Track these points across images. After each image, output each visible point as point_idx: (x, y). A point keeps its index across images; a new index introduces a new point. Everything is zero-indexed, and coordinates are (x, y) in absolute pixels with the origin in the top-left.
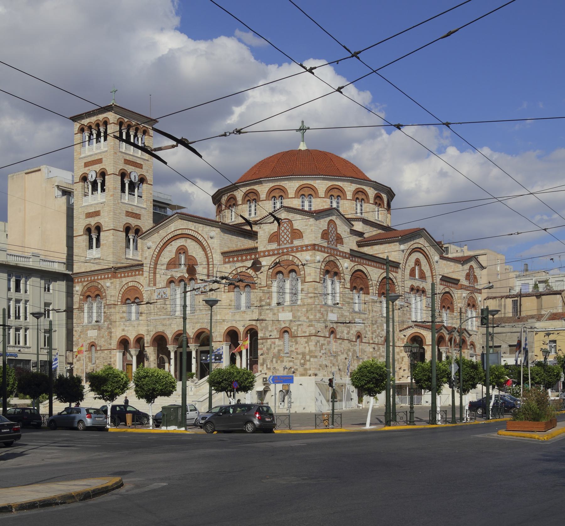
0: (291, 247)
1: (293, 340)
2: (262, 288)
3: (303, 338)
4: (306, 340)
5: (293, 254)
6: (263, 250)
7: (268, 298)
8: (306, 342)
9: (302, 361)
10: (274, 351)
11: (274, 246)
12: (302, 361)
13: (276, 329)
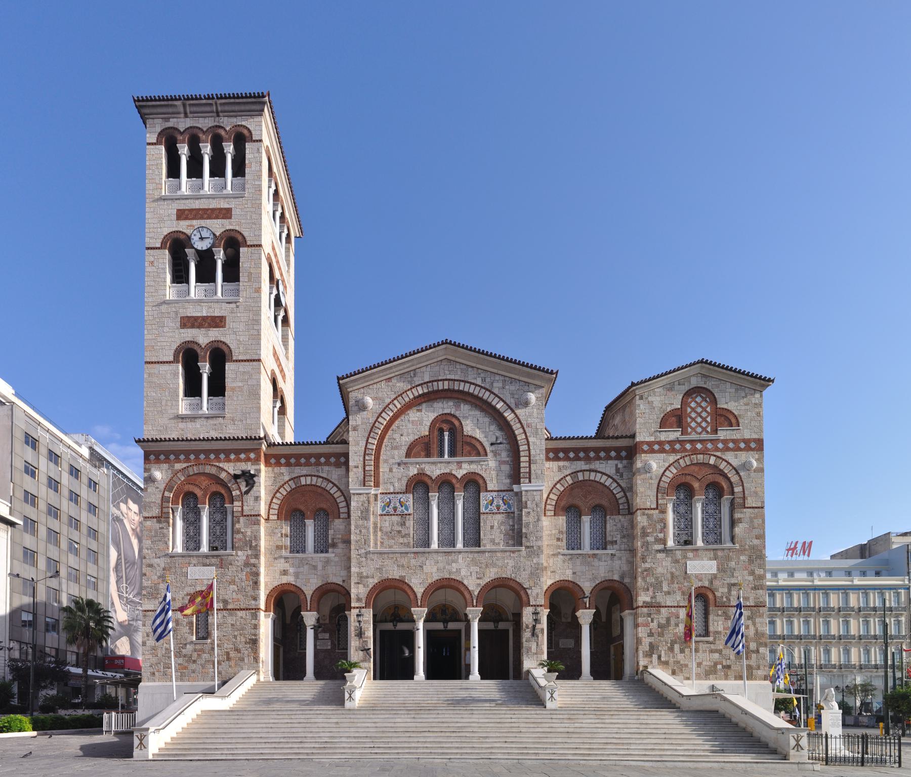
1: (720, 613)
5: (718, 454)
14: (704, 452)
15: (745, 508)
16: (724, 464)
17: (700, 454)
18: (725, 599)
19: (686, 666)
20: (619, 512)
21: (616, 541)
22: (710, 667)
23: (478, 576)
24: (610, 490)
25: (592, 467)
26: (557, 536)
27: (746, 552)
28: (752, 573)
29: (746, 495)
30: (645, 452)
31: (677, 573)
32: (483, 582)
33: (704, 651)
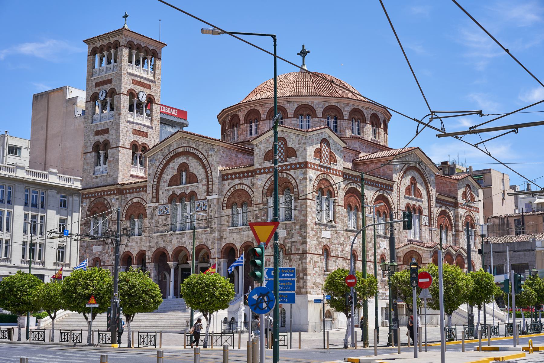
2: (258, 206)
4: (298, 257)
5: (288, 172)
8: (300, 260)
18: (289, 250)
27: (299, 224)
28: (301, 235)
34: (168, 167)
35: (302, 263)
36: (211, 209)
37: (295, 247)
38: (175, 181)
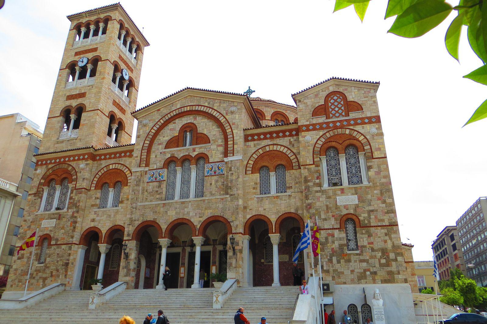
0: (346, 120)
1: (364, 232)
2: (307, 167)
3: (379, 228)
4: (384, 231)
5: (351, 127)
6: (305, 124)
7: (318, 178)
8: (386, 235)
9: (383, 261)
10: (334, 246)
11: (322, 119)
12: (383, 261)
13: (333, 216)
14: (342, 127)
15: (373, 159)
16: (356, 133)
17: (339, 128)
18: (366, 222)
19: (343, 273)
20: (293, 168)
21: (292, 187)
22: (361, 273)
23: (200, 216)
24: (286, 155)
25: (275, 142)
26: (253, 186)
27: (378, 188)
28: (384, 202)
29: (373, 150)
30: (303, 131)
31: (331, 206)
32: (202, 220)
33: (355, 261)
34: (166, 128)
35: (391, 239)
36: (231, 172)
37: (376, 217)
38: (174, 142)
